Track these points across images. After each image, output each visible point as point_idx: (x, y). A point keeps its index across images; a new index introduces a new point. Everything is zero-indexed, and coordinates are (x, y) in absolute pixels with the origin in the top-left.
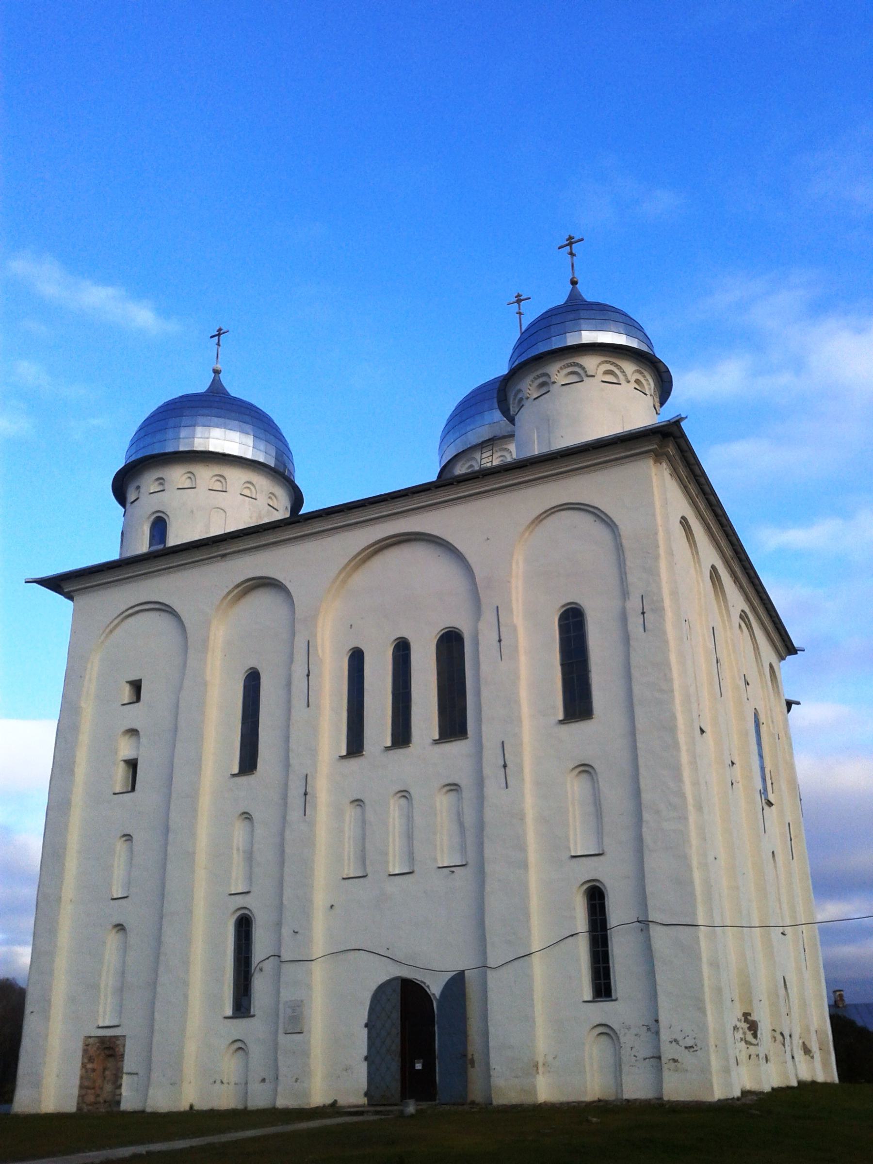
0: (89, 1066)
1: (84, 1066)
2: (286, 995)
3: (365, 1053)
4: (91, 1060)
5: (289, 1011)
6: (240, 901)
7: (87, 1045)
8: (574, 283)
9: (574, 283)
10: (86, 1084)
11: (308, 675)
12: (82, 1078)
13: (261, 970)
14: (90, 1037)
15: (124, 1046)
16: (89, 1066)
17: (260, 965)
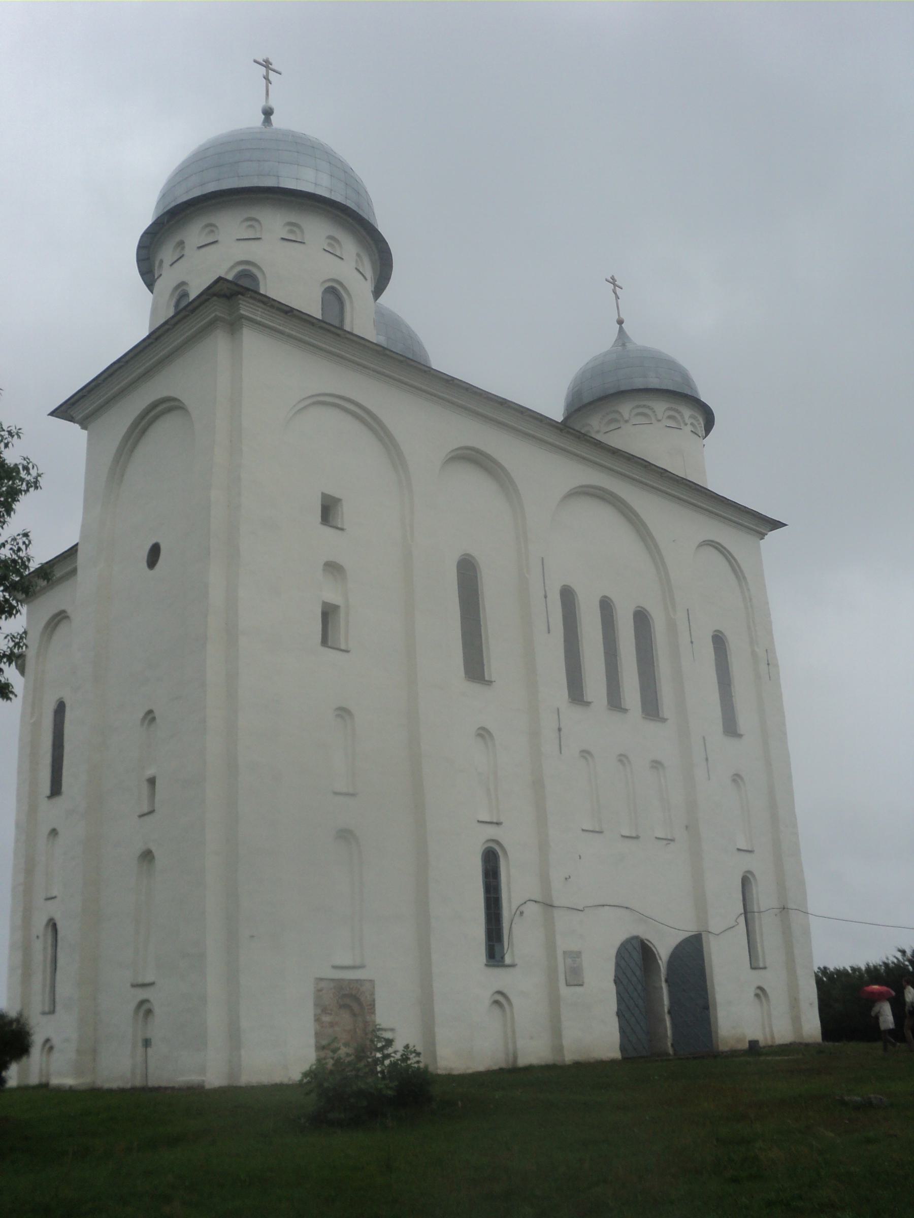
0: (326, 1019)
1: (317, 1020)
2: (563, 944)
3: (614, 1007)
4: (325, 1010)
5: (569, 961)
6: (491, 832)
7: (320, 990)
8: (620, 322)
9: (620, 322)
10: (324, 1042)
11: (546, 597)
12: (317, 1035)
13: (522, 913)
14: (321, 979)
15: (373, 994)
16: (326, 1019)
17: (521, 909)
